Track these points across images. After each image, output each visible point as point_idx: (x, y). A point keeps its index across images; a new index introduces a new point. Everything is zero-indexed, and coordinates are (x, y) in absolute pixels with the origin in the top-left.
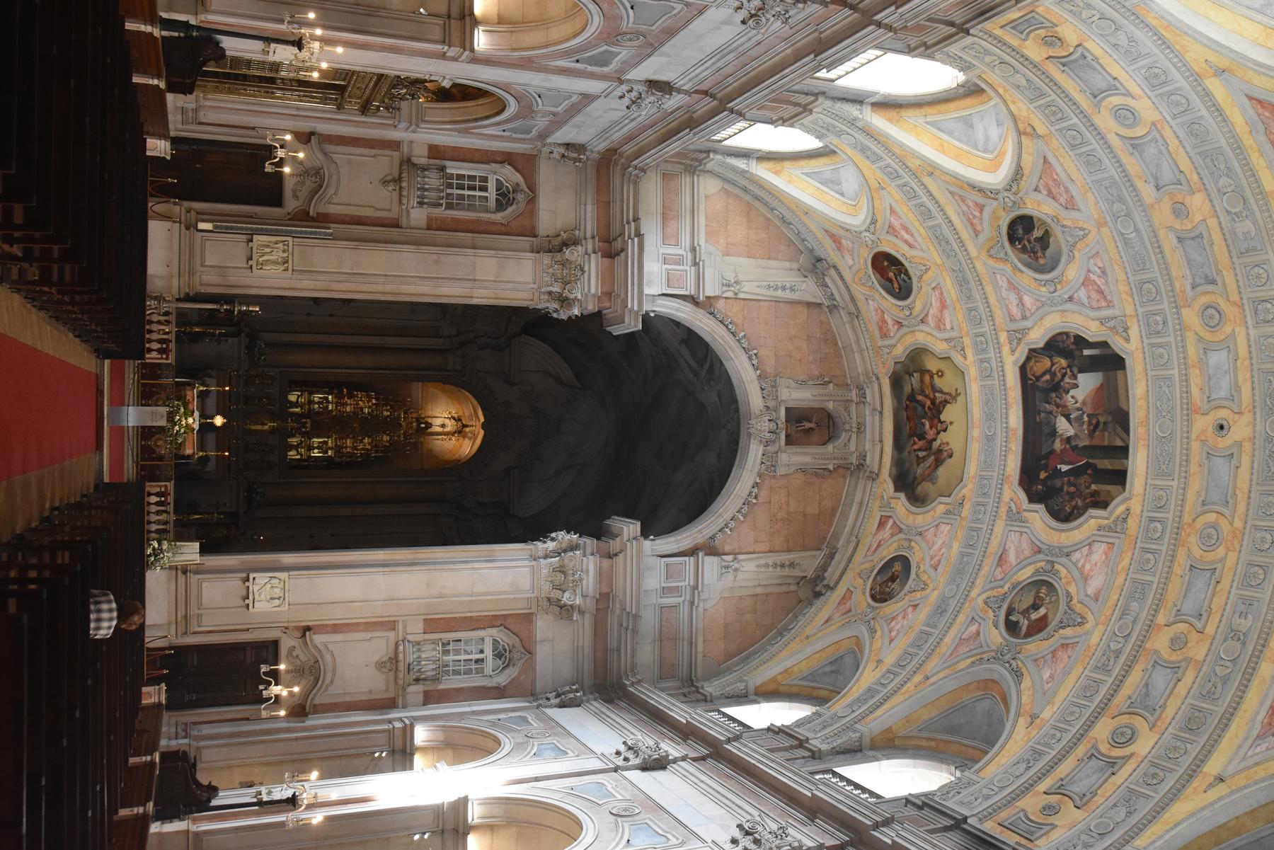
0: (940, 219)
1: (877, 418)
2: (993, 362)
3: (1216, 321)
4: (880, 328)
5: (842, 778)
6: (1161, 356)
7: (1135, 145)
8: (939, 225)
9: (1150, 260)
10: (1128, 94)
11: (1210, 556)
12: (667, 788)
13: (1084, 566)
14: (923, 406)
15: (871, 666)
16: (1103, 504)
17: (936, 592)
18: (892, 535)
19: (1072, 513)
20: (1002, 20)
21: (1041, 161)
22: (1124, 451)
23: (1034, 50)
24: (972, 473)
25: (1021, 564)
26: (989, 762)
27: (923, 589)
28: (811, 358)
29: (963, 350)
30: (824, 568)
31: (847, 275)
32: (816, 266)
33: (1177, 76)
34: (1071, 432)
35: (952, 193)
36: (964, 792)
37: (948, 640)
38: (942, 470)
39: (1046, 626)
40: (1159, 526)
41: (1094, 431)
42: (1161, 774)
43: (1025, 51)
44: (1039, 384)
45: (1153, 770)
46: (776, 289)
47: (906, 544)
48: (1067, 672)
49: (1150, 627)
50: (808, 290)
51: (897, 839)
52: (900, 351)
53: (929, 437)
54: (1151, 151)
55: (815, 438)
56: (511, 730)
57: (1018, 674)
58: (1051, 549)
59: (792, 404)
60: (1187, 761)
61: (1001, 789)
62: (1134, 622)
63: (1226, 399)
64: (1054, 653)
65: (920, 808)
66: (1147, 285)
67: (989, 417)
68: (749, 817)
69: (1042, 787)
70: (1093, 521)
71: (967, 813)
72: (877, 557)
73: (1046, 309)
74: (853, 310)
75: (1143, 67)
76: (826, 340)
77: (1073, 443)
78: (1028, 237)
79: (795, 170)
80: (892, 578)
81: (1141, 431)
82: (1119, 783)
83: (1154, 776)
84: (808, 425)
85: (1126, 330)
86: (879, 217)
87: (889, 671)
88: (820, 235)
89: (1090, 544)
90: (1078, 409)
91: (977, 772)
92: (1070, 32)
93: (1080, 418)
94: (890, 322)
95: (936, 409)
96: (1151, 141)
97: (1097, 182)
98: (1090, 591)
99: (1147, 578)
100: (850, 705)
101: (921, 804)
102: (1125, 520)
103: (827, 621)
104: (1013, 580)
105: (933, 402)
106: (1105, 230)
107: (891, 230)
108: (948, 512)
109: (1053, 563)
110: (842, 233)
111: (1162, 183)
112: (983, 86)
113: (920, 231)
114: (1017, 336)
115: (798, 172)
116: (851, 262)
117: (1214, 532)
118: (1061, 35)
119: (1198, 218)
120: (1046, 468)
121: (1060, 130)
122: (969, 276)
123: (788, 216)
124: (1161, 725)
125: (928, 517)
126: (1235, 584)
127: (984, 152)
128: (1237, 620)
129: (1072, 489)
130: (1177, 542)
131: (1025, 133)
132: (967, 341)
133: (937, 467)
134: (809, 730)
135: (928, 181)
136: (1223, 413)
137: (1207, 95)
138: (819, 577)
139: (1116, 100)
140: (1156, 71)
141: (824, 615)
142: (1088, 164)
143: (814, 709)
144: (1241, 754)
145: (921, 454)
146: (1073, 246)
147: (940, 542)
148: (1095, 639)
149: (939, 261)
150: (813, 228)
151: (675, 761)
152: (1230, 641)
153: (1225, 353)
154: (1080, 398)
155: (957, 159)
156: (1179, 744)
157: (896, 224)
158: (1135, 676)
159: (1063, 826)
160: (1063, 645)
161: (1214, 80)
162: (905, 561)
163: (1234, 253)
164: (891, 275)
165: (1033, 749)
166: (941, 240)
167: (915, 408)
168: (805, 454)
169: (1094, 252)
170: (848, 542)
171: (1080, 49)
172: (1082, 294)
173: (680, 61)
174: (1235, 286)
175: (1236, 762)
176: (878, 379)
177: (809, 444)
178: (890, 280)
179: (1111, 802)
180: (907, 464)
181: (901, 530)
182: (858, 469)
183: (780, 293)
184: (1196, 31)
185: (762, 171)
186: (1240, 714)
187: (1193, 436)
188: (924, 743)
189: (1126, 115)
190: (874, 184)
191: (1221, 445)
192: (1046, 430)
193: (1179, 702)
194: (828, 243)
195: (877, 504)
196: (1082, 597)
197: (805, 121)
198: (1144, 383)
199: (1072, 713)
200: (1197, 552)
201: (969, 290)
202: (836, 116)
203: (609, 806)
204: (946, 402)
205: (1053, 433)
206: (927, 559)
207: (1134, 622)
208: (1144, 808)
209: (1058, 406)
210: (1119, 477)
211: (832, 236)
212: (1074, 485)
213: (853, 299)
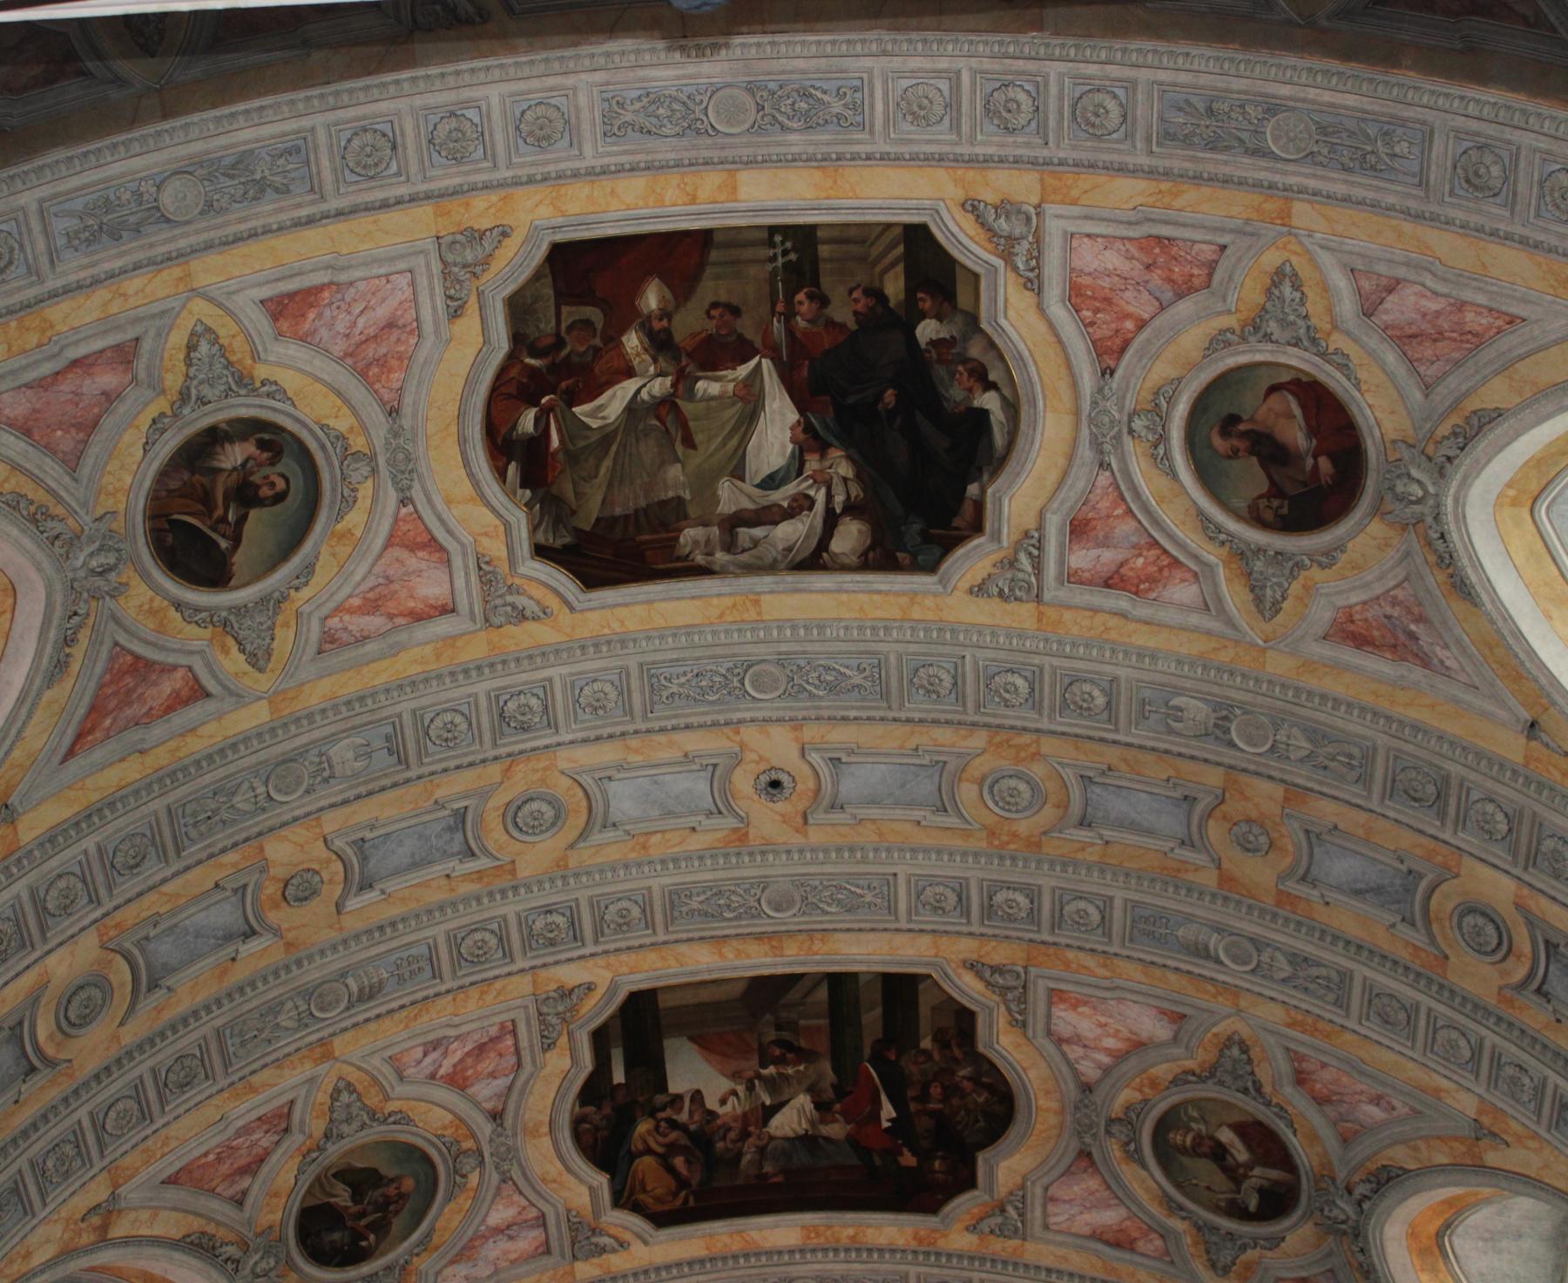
7: (149, 980)
10: (34, 999)
16: (962, 1022)
21: (172, 1194)
25: (1117, 1193)
54: (165, 950)
89: (1060, 1041)
96: (143, 951)
97: (227, 1064)
119: (319, 850)
131: (104, 1228)
136: (743, 782)
153: (612, 787)
163: (400, 778)
187: (797, 840)
198: (683, 948)
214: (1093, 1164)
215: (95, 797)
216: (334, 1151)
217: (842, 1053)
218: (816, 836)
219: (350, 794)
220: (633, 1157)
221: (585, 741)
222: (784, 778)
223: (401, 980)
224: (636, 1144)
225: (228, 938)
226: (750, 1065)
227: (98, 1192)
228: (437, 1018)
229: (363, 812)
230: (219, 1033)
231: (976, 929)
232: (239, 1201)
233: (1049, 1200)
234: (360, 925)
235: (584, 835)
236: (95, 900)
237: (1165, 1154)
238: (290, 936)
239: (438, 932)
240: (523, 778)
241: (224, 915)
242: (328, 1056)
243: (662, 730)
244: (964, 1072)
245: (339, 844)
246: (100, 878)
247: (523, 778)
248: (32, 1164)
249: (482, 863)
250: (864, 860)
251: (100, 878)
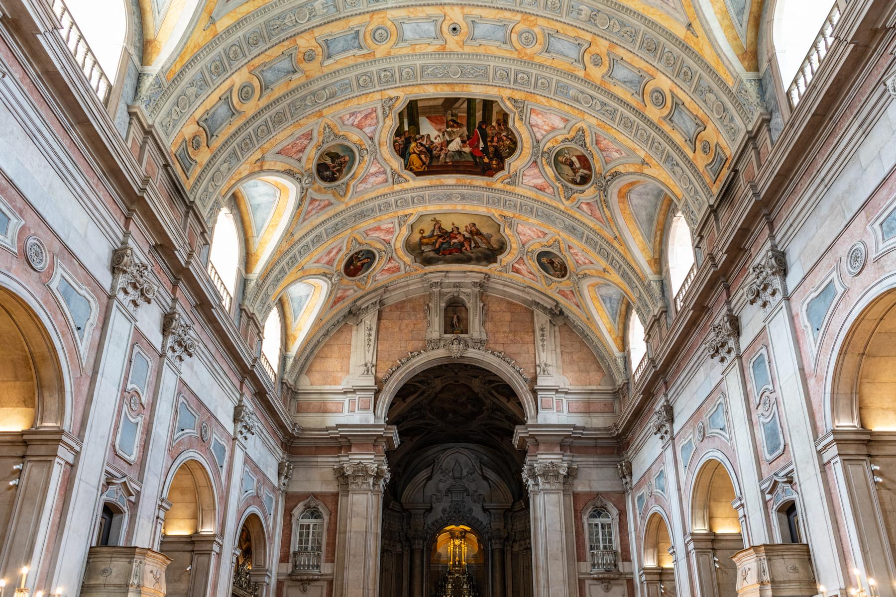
0: (321, 229)
1: (450, 274)
2: (414, 194)
3: (383, 32)
4: (394, 272)
5: (678, 294)
6: (408, 73)
7: (265, 87)
8: (326, 230)
9: (343, 79)
10: (231, 90)
11: (540, 37)
12: (686, 405)
13: (545, 130)
14: (442, 243)
15: (607, 276)
16: (504, 118)
17: (561, 233)
18: (524, 264)
19: (510, 139)
20: (182, 178)
21: (280, 156)
22: (470, 101)
23: (203, 156)
24: (485, 210)
25: (543, 174)
26: (673, 192)
27: (559, 242)
28: (413, 318)
29: (406, 216)
30: (544, 308)
31: (360, 293)
32: (354, 314)
33: (216, 52)
34: (458, 140)
35: (304, 220)
36: (692, 208)
37: (591, 225)
38: (484, 231)
39: (584, 156)
40: (519, 76)
41: (457, 123)
42: (685, 69)
43: (205, 161)
44: (427, 162)
45: (682, 76)
46: (370, 340)
47: (530, 254)
48: (615, 140)
49: (585, 81)
50: (370, 320)
51: (724, 251)
52: (408, 259)
53: (462, 240)
54: (269, 75)
55: (464, 315)
56: (647, 504)
57: (616, 175)
58: (534, 154)
59: (442, 330)
60: (677, 51)
61: (691, 182)
62: (582, 93)
63: (435, 26)
64: (602, 150)
65: (702, 237)
66: (361, 82)
67: (449, 197)
68: (707, 351)
69: (690, 154)
70: (516, 124)
71: (706, 206)
72: (538, 274)
73: (378, 156)
75: (211, 78)
76: (402, 308)
77: (465, 138)
78: (332, 167)
79: (293, 327)
80: (551, 263)
81: (457, 89)
82: (689, 99)
83: (685, 74)
84: (455, 320)
85: (391, 99)
86: (322, 271)
87: (611, 264)
88: (334, 311)
90: (444, 135)
91: (679, 200)
92: (190, 130)
93: (450, 134)
94: (390, 265)
95: (445, 235)
96: (262, 75)
97: (292, 116)
98: (561, 125)
99: (554, 84)
100: (632, 288)
101: (699, 236)
102: (515, 101)
103: (578, 306)
104: (554, 180)
105: (440, 237)
106: (324, 112)
107: (330, 263)
108: (510, 226)
109: (543, 153)
110: (333, 296)
111: (291, 69)
112: (230, 194)
113: (329, 244)
114: (396, 177)
115: (294, 325)
116: (352, 291)
117: (524, 35)
118: (191, 136)
119: (314, 43)
120: (482, 158)
121: (258, 141)
122: (358, 210)
123: (321, 333)
124: (652, 70)
125: (513, 240)
126: (559, 19)
127: (275, 197)
128: (583, 17)
129: (495, 139)
130: (530, 62)
131: (261, 166)
132: (401, 213)
133: (481, 234)
134: (648, 315)
135: (297, 236)
136: (445, 28)
137: (228, 31)
138: (551, 312)
139: (235, 100)
140: (213, 68)
141: (574, 308)
142: (280, 122)
143: (634, 312)
144: (672, 12)
145: (473, 245)
146: (336, 135)
147: (529, 232)
148: (594, 121)
149: (349, 231)
150: (330, 316)
151: (667, 401)
152: (597, 22)
153: (404, 26)
154: (437, 133)
155: (280, 216)
156: (665, 57)
157: (326, 259)
158: (619, 91)
159: (718, 138)
160: (597, 144)
161: (218, 24)
162: (541, 255)
164: (359, 264)
165: (665, 162)
166: (336, 229)
167: (444, 249)
168: (473, 321)
169: (339, 121)
170: (528, 293)
171: (201, 123)
172: (368, 130)
173: (220, 398)
174: (360, 17)
175: (677, 15)
176: (425, 274)
177: (467, 319)
178: (363, 264)
179: (702, 104)
180: (480, 255)
181: (521, 258)
182: (483, 287)
183: (372, 338)
184: (183, 36)
185: (294, 348)
186: (645, 14)
187: (460, 50)
188: (658, 239)
189: (245, 93)
190: (300, 274)
191: (466, 30)
192: (457, 158)
193: (636, 58)
194: (340, 306)
195: (504, 275)
196: (565, 131)
197: (260, 319)
198: (425, 87)
199: (642, 135)
200: (538, 48)
201: (368, 210)
202: (256, 296)
203: (697, 442)
204: (439, 228)
205: (459, 153)
206: (540, 240)
207: (582, 93)
208: (708, 80)
209: (441, 149)
210: (488, 105)
211: (335, 303)
212: (493, 138)
213: (375, 290)
214: (537, 165)
215: (240, 16)
216: (325, 146)
217: (469, 125)
218: (467, 49)
219: (322, 22)
220: (410, 154)
221: (396, 7)
222: (458, 27)
223: (342, 91)
224: (411, 150)
225: (288, 72)
226: (444, 127)
227: (258, 155)
228: (353, 105)
229: (327, 30)
230: (289, 105)
231: (512, 86)
232: (299, 160)
233: (523, 175)
234: (328, 72)
235: (396, 44)
236: (244, 55)
237: (557, 164)
238: (307, 73)
239: (352, 75)
240: (376, 21)
241: (286, 64)
242: (321, 116)
243: (420, 5)
244: (504, 134)
245: (320, 41)
246: (245, 48)
247: (376, 21)
248: (238, 145)
249: (365, 51)
250: (480, 60)
251: (245, 48)
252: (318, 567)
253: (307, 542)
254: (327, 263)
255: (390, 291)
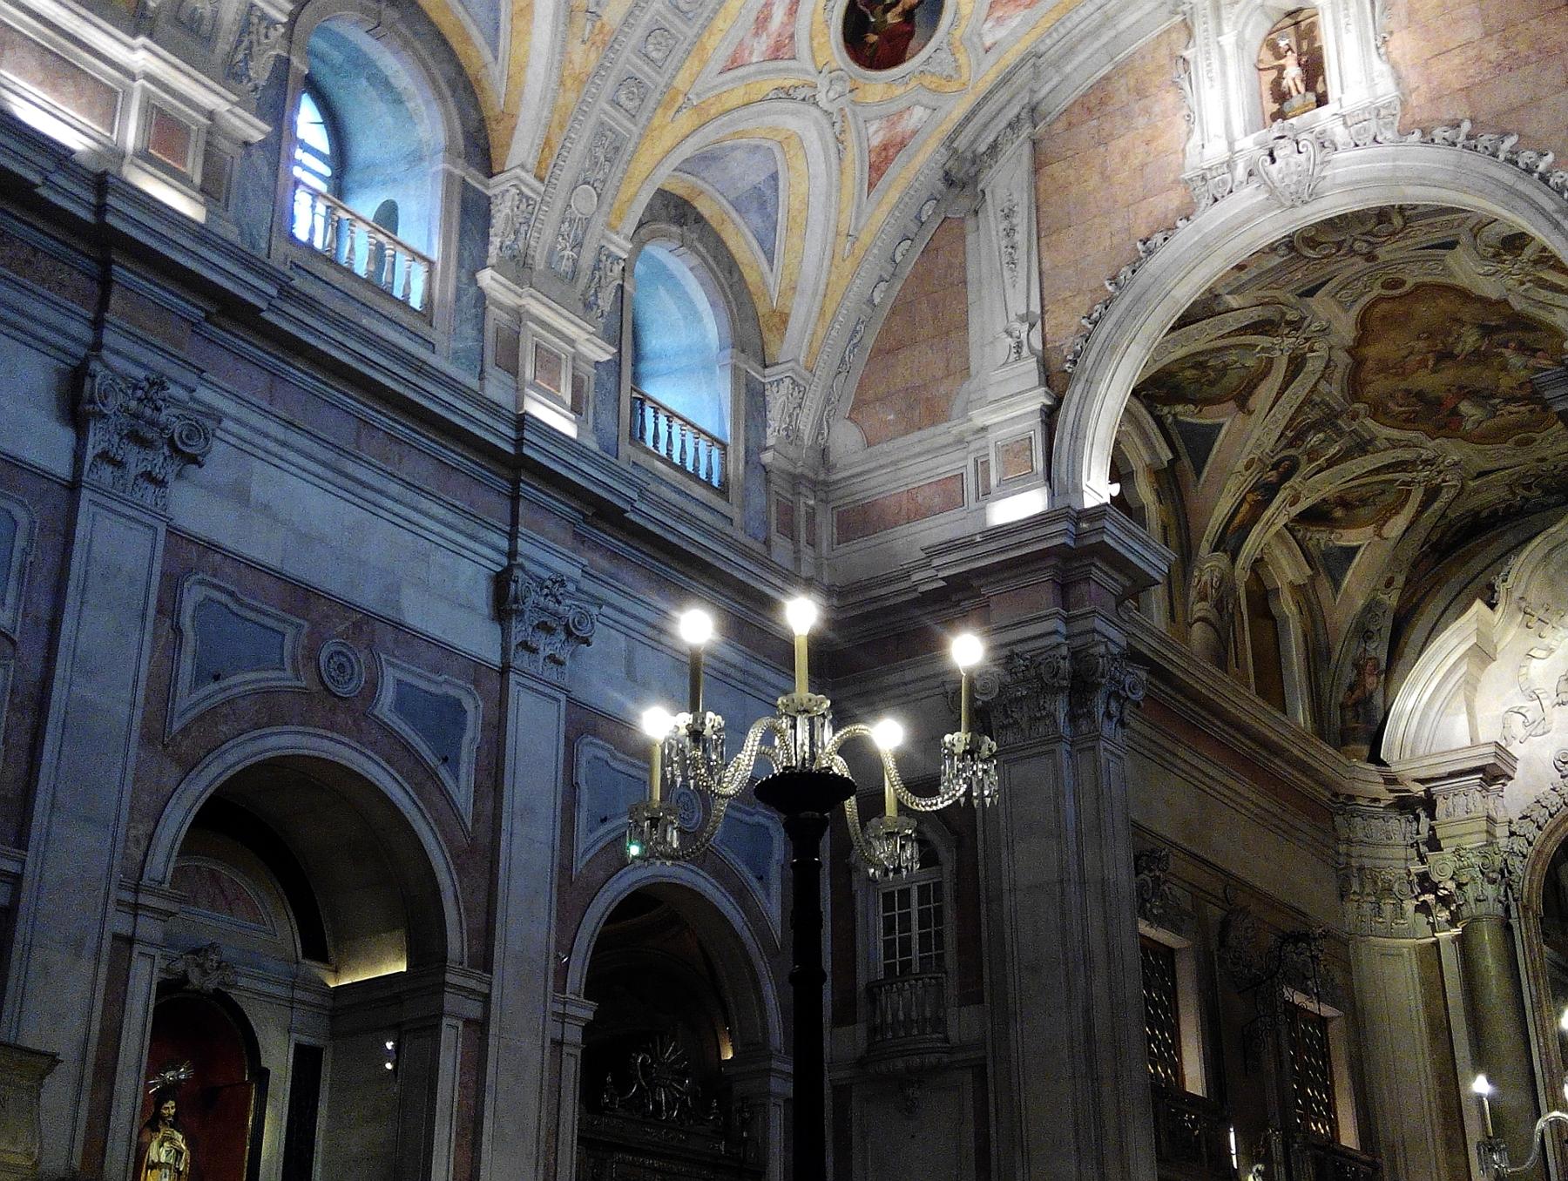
74: (1026, 73)
110: (852, 152)
150: (881, 215)
178: (908, 15)
252: (939, 1023)
253: (906, 948)
254: (776, 53)
255: (1056, 65)
